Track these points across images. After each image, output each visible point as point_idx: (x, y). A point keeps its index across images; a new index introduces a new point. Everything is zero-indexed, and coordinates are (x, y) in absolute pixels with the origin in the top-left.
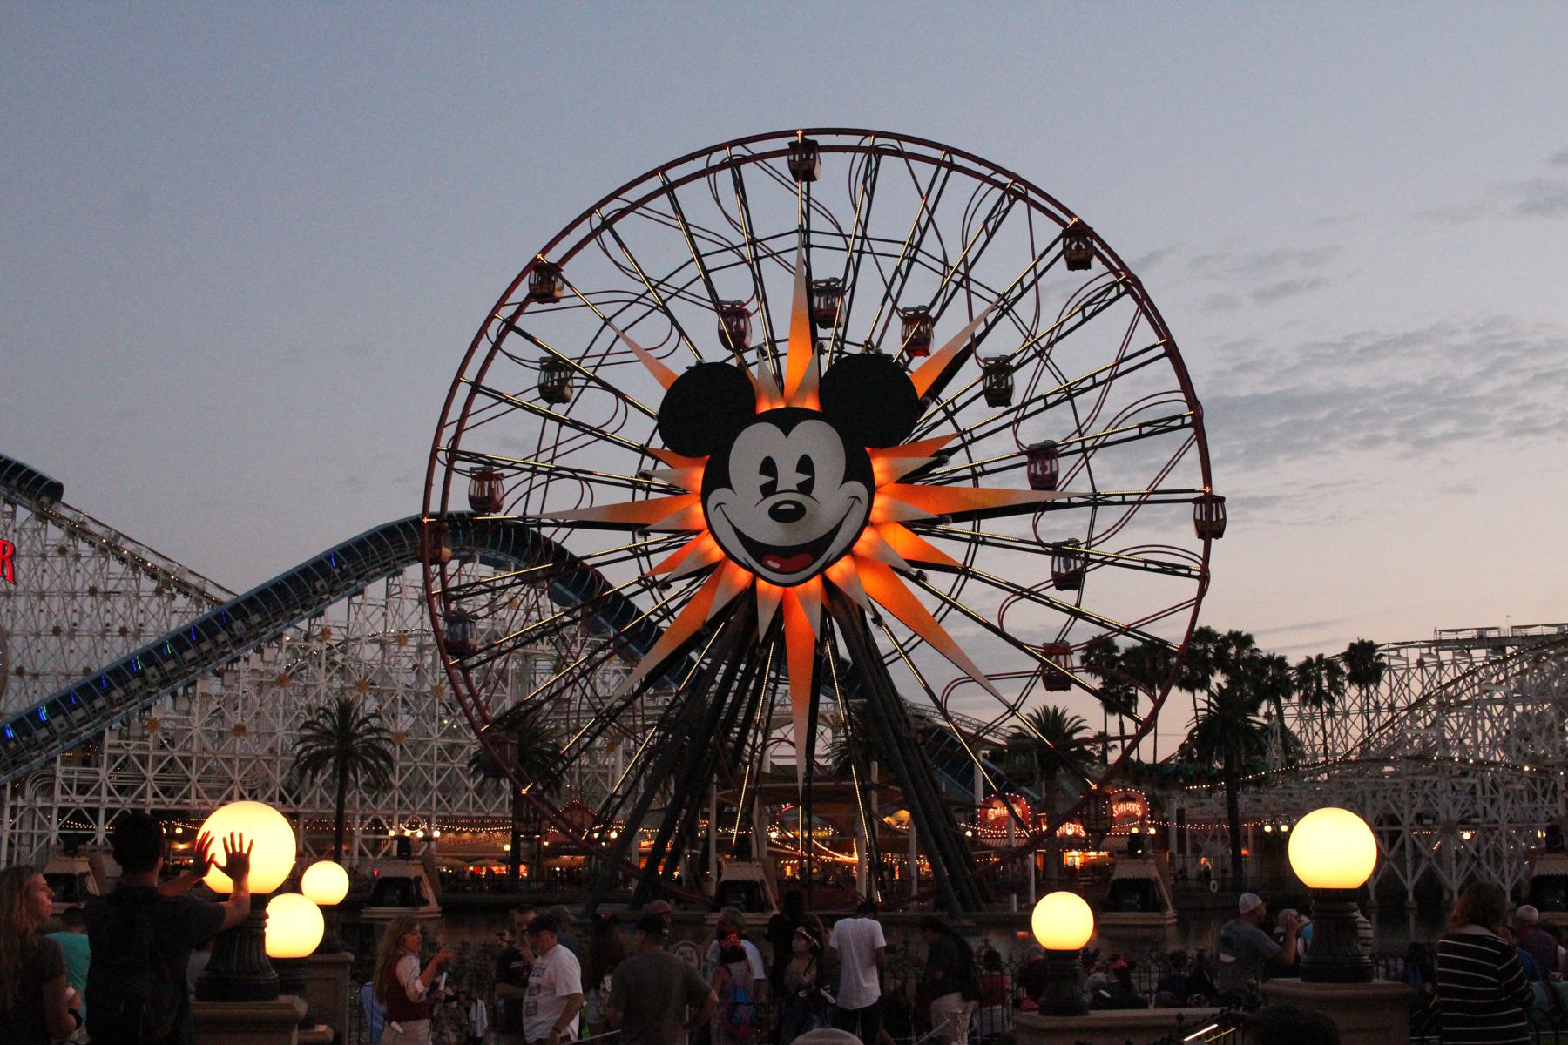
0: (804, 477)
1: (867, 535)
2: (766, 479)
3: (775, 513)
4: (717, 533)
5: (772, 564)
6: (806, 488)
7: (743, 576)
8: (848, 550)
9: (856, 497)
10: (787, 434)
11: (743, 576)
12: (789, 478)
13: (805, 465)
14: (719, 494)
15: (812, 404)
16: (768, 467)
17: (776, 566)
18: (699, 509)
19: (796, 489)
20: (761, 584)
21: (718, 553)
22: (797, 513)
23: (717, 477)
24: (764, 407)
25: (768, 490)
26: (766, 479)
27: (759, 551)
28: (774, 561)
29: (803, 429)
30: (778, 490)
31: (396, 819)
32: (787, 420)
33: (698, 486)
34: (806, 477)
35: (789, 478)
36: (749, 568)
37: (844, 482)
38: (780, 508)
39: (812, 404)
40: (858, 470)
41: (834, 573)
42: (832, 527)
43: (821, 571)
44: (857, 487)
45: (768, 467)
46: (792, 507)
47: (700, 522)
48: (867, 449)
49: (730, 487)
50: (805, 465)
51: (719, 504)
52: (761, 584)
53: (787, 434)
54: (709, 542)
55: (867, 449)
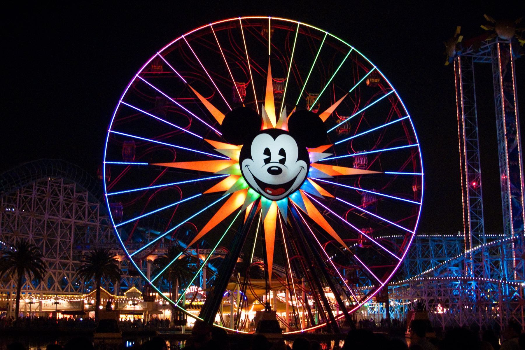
0: (282, 157)
1: (305, 183)
2: (267, 157)
3: (270, 171)
4: (246, 177)
5: (268, 191)
6: (282, 162)
7: (256, 195)
8: (298, 188)
9: (302, 167)
10: (275, 139)
11: (256, 195)
12: (276, 157)
13: (282, 152)
14: (246, 161)
15: (285, 128)
16: (267, 152)
17: (270, 192)
18: (237, 166)
19: (278, 162)
20: (263, 199)
21: (245, 185)
22: (279, 171)
23: (246, 154)
24: (265, 128)
25: (267, 161)
26: (267, 157)
27: (263, 186)
28: (269, 190)
29: (282, 138)
30: (271, 161)
31: (27, 293)
32: (275, 133)
33: (237, 157)
34: (282, 157)
35: (276, 157)
36: (259, 193)
37: (298, 160)
38: (272, 169)
39: (285, 128)
40: (303, 156)
41: (293, 196)
42: (293, 178)
43: (287, 196)
44: (303, 163)
45: (267, 152)
46: (277, 169)
47: (239, 172)
48: (307, 148)
49: (251, 158)
50: (282, 152)
51: (247, 165)
52: (263, 199)
53: (275, 139)
54: (242, 180)
55: (307, 148)
